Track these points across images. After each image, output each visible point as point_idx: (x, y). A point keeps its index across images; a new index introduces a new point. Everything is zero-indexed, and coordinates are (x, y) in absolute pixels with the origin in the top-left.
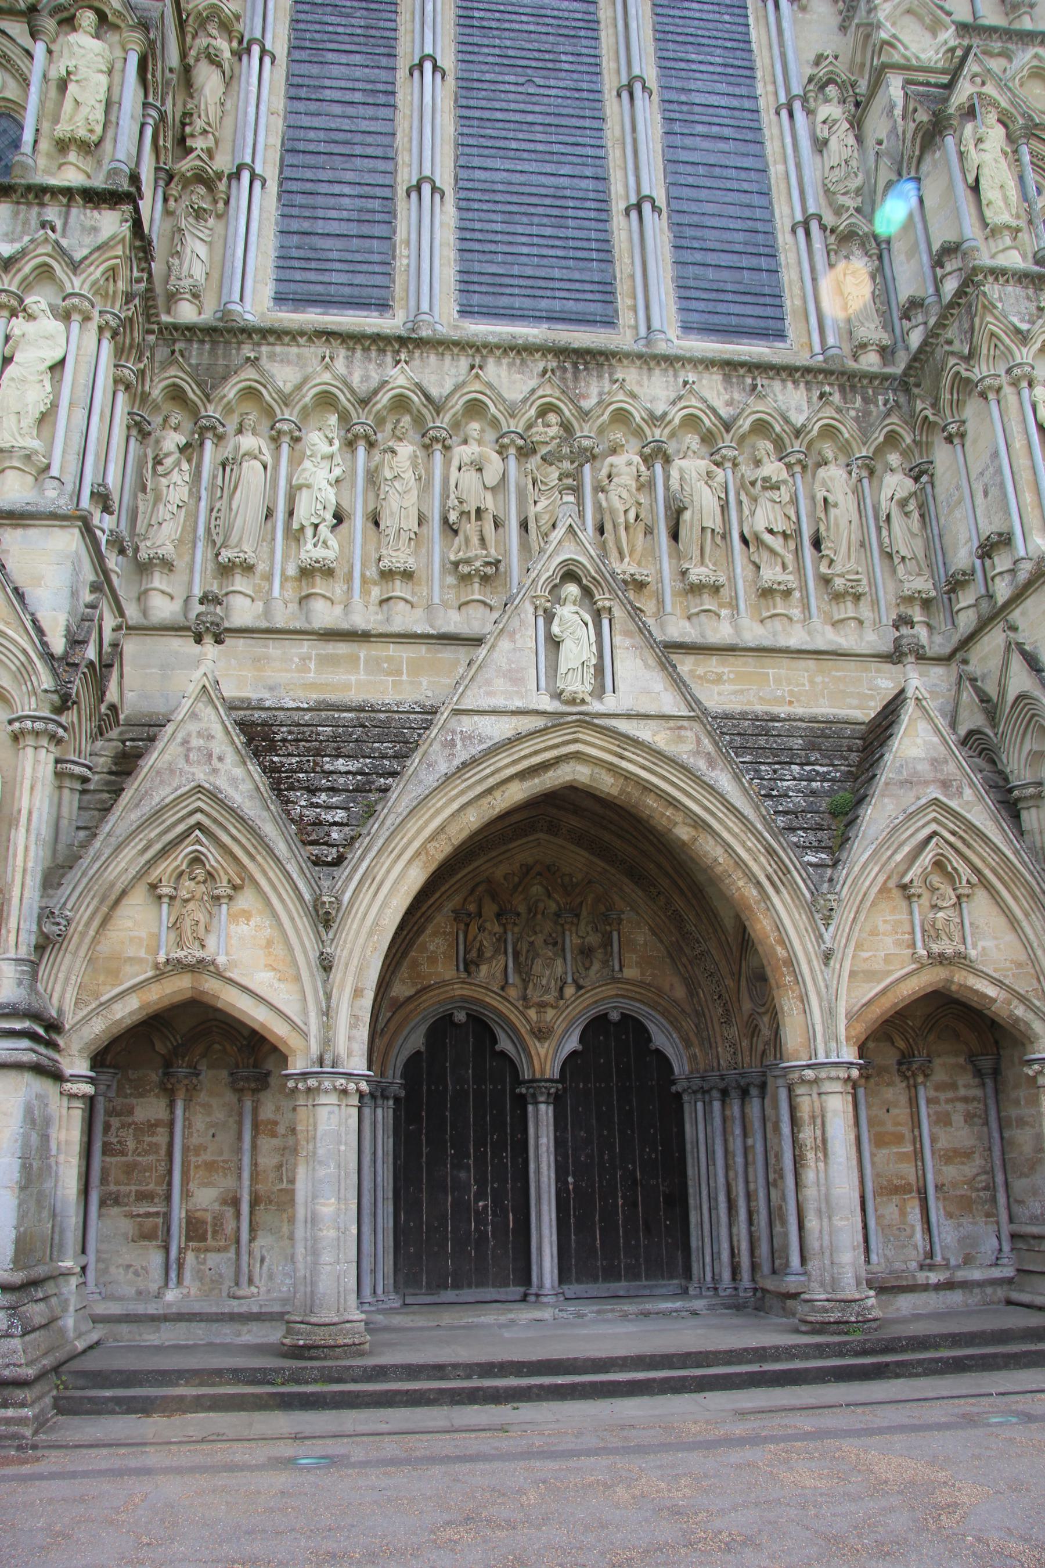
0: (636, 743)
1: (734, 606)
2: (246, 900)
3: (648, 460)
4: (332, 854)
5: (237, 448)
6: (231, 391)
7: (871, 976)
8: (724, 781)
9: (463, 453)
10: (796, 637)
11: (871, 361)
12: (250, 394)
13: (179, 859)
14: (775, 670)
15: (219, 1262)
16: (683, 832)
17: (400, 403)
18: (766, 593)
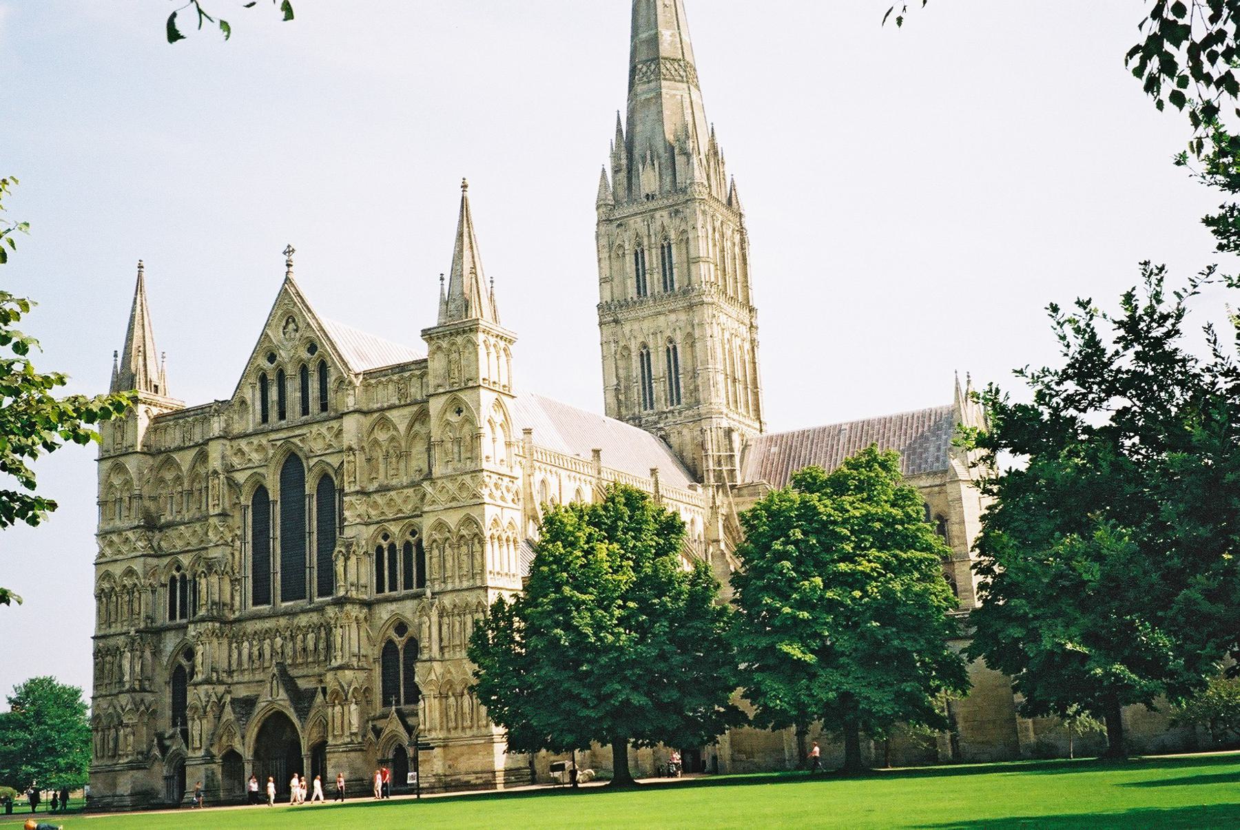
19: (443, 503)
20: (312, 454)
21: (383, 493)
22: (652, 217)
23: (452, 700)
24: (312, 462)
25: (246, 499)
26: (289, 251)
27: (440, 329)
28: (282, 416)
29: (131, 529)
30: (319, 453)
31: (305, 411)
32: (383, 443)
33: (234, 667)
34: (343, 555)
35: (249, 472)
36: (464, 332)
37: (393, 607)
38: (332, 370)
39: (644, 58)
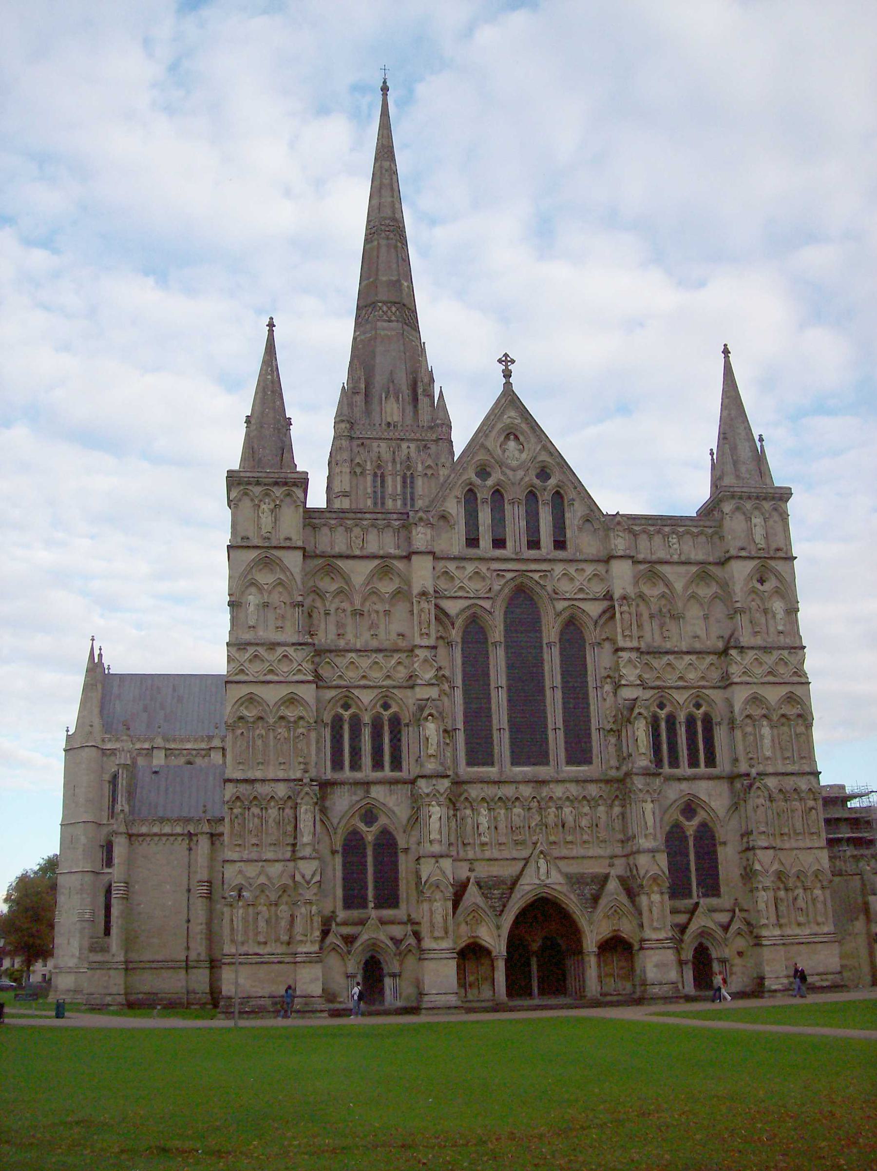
0: (555, 890)
1: (577, 845)
2: (483, 923)
3: (557, 808)
4: (499, 913)
5: (465, 814)
6: (462, 798)
7: (601, 934)
8: (572, 896)
9: (517, 810)
10: (591, 853)
11: (613, 773)
12: (466, 798)
13: (471, 917)
14: (585, 861)
15: (475, 991)
16: (564, 906)
17: (500, 798)
18: (584, 842)
19: (758, 676)
20: (556, 596)
21: (657, 656)
22: (399, 446)
23: (782, 894)
24: (561, 605)
25: (455, 634)
26: (506, 361)
27: (744, 490)
28: (499, 543)
29: (293, 644)
30: (568, 596)
31: (534, 544)
32: (652, 599)
33: (453, 840)
34: (645, 718)
35: (462, 604)
36: (773, 498)
37: (684, 786)
38: (576, 504)
39: (384, 299)
